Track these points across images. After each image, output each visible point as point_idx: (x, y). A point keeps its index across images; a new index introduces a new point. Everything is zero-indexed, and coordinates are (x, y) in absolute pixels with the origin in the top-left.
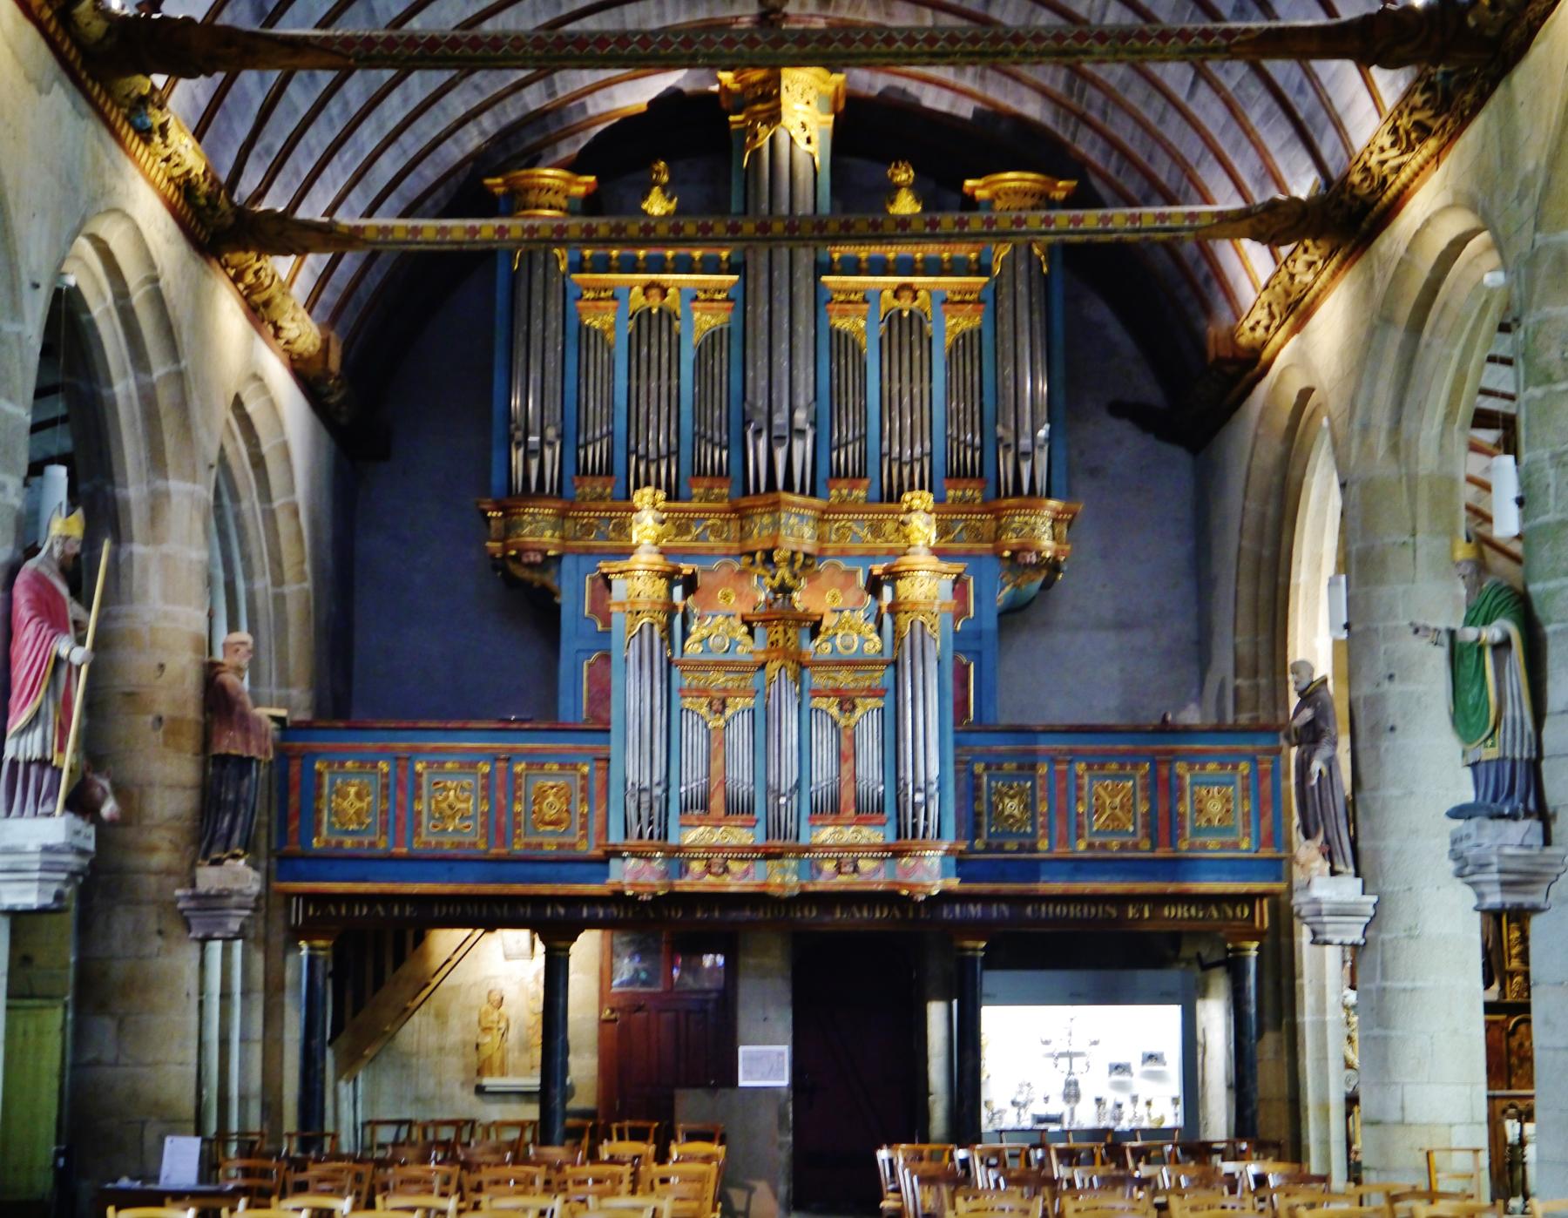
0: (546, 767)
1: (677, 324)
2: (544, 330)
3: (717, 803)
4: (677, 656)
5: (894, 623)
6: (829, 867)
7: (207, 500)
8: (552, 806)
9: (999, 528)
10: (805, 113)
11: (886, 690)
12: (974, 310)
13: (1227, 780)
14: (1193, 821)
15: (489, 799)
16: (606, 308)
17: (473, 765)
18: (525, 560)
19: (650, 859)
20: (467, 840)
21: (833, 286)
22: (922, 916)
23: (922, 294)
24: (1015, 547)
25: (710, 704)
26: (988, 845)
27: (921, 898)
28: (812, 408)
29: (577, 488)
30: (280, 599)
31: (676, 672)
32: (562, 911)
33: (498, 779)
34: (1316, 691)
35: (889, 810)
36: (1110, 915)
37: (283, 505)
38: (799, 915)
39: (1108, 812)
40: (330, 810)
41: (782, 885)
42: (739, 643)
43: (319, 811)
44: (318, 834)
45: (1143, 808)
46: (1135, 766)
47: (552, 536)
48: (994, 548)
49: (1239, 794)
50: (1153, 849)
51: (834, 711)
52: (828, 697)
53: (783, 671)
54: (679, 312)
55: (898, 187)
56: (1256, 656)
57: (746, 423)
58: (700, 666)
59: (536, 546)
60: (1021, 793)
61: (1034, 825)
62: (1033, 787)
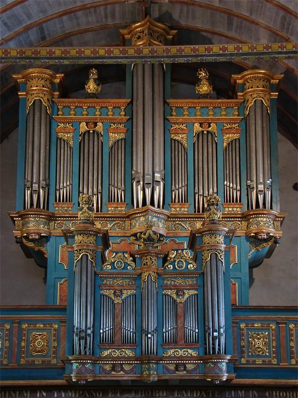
0: (37, 326)
1: (101, 138)
8: (39, 343)
9: (248, 224)
18: (30, 237)
25: (115, 293)
26: (247, 361)
28: (163, 172)
29: (55, 207)
33: (15, 331)
42: (129, 265)
47: (44, 227)
51: (175, 296)
52: (171, 289)
54: (102, 133)
55: (200, 80)
57: (133, 179)
58: (110, 275)
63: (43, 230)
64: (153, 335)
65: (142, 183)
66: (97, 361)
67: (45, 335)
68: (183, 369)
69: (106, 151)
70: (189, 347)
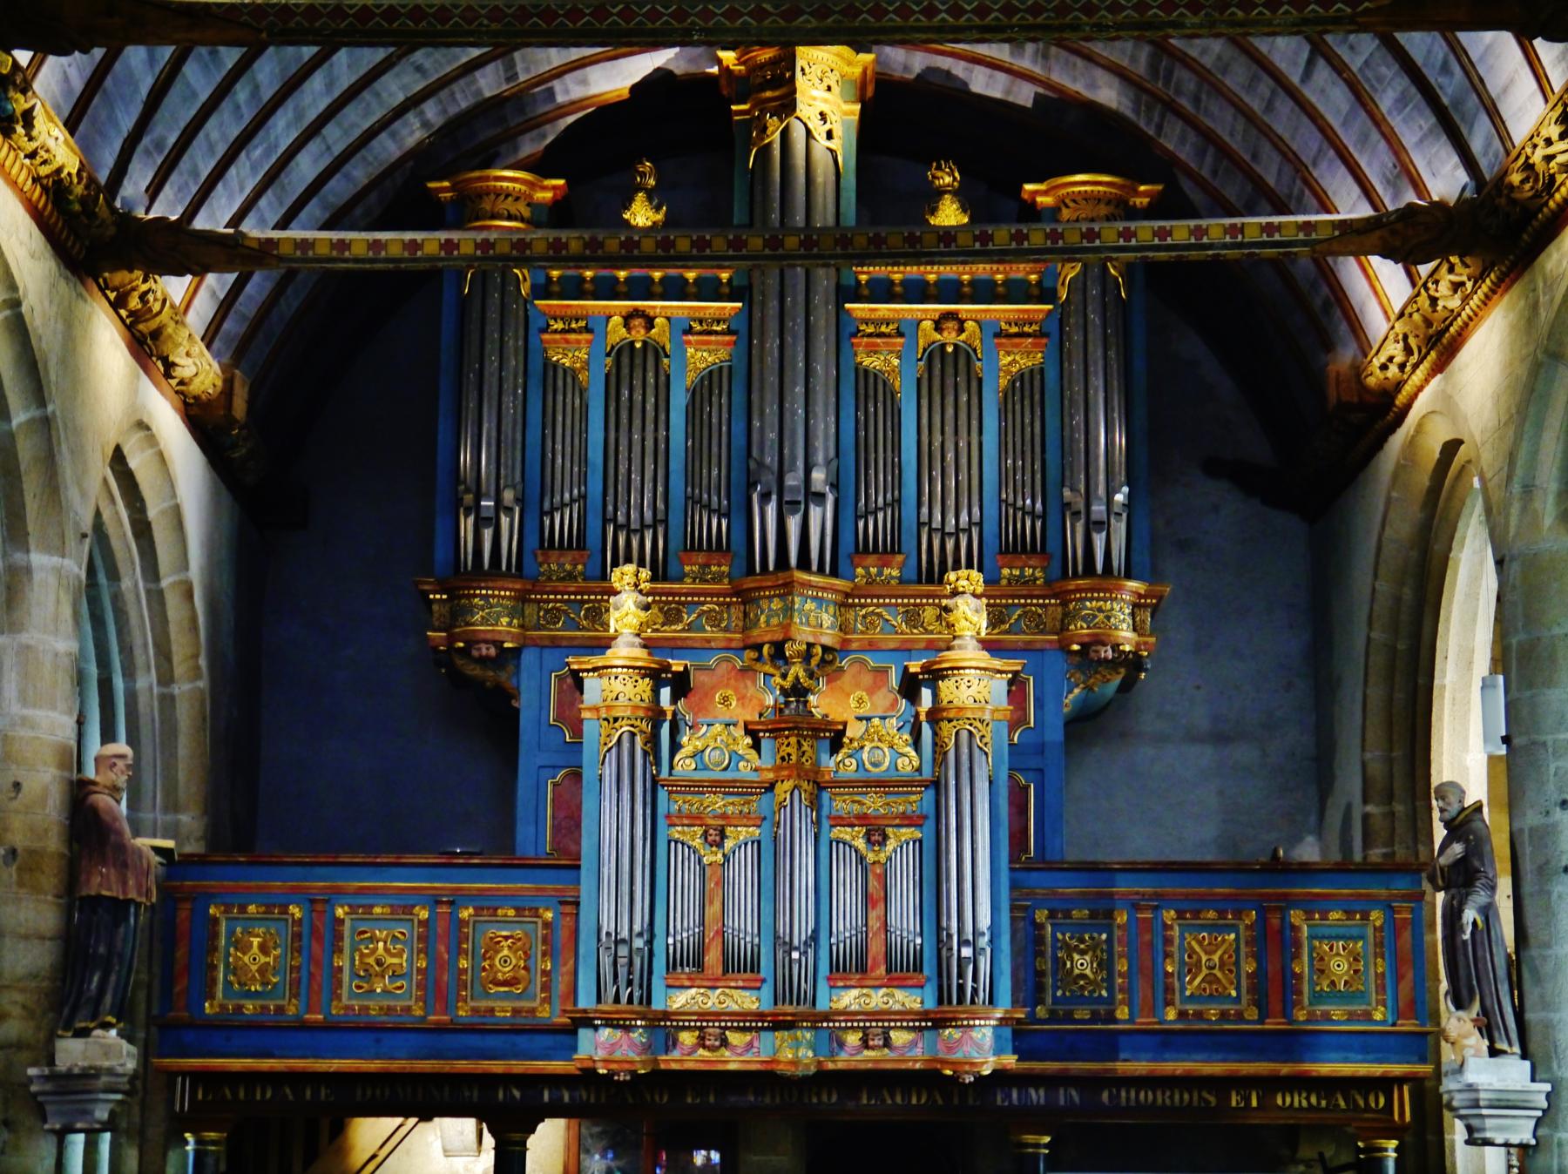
0: (500, 912)
2: (501, 369)
3: (713, 958)
4: (664, 774)
5: (935, 734)
6: (853, 1039)
7: (78, 577)
9: (1066, 615)
10: (825, 101)
11: (925, 817)
12: (1034, 345)
13: (1355, 932)
14: (1313, 983)
15: (426, 954)
16: (578, 342)
17: (408, 909)
18: (475, 653)
19: (628, 1029)
20: (400, 1004)
21: (859, 314)
22: (971, 1101)
23: (970, 325)
24: (1086, 639)
25: (705, 835)
26: (1052, 1012)
27: (969, 1079)
28: (834, 464)
29: (541, 565)
30: (168, 701)
31: (662, 794)
32: (517, 1094)
34: (1468, 820)
35: (929, 969)
36: (1207, 1102)
37: (174, 584)
38: (815, 1100)
39: (1205, 971)
40: (227, 964)
41: (795, 1062)
42: (742, 758)
43: (215, 968)
44: (212, 997)
45: (1249, 967)
46: (1238, 915)
47: (510, 624)
48: (1059, 641)
49: (1371, 949)
50: (1261, 1021)
51: (860, 843)
52: (852, 826)
53: (796, 792)
54: (668, 347)
55: (940, 193)
56: (1391, 776)
57: (751, 485)
58: (695, 787)
59: (489, 636)
60: (1094, 948)
61: (1110, 990)
62: (1109, 941)
63: (509, 632)
64: (806, 952)
65: (774, 497)
66: (660, 1020)
67: (520, 939)
68: (881, 1043)
69: (679, 401)
70: (895, 983)
